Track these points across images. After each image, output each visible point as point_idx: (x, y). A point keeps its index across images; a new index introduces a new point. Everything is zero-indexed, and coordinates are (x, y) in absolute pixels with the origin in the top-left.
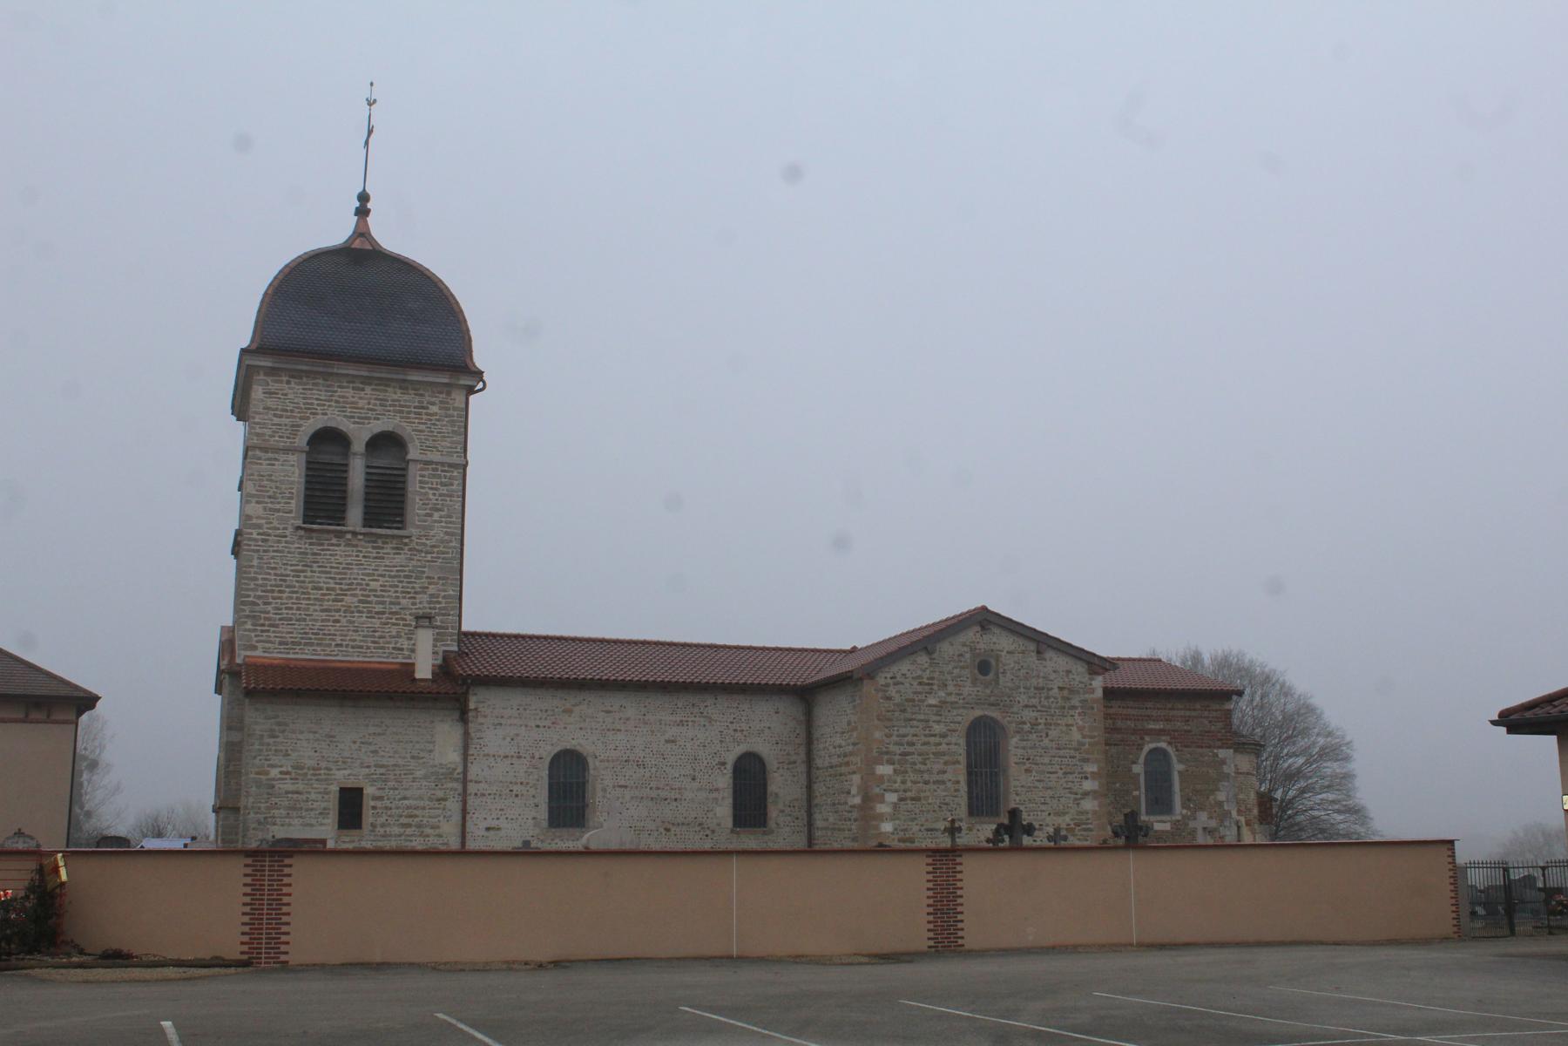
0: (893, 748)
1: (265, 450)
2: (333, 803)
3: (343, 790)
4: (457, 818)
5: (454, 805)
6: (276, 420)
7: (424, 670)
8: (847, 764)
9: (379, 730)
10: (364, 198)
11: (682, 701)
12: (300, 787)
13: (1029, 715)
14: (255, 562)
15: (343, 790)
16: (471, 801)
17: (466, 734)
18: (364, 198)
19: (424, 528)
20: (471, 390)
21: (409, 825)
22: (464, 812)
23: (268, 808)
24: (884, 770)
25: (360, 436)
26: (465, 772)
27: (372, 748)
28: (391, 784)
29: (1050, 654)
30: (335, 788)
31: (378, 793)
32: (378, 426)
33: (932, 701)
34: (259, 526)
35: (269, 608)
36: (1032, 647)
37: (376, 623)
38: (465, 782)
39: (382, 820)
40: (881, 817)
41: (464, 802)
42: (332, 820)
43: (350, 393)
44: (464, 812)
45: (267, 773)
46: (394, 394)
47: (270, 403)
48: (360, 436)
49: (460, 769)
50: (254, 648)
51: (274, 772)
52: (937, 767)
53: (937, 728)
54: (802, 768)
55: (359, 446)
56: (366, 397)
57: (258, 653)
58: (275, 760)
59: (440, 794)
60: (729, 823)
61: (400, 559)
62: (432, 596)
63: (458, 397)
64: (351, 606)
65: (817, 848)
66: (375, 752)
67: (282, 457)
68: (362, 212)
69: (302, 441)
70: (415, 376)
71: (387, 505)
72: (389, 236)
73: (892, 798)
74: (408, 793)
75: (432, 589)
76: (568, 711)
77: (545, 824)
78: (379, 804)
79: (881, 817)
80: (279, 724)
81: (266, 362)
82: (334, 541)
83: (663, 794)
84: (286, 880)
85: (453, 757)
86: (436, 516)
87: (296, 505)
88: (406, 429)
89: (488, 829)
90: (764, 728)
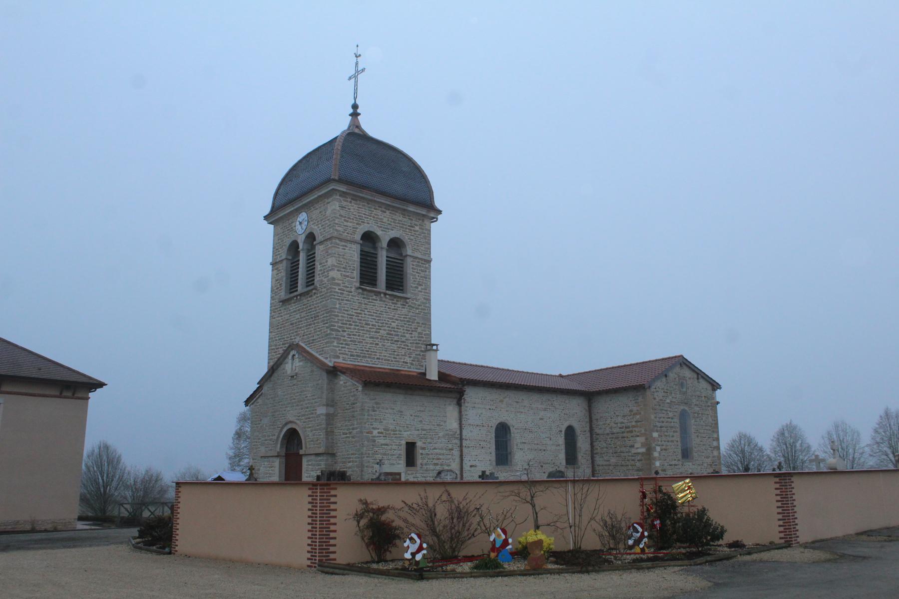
0: (658, 424)
1: (341, 240)
2: (403, 452)
3: (407, 443)
4: (458, 460)
5: (456, 453)
6: (345, 223)
7: (433, 375)
8: (631, 432)
9: (422, 409)
10: (355, 107)
11: (545, 397)
12: (387, 441)
13: (697, 409)
14: (337, 306)
15: (407, 443)
16: (464, 450)
17: (460, 412)
18: (355, 107)
19: (415, 294)
20: (434, 219)
21: (437, 464)
22: (461, 456)
23: (373, 454)
24: (655, 435)
25: (385, 238)
26: (461, 434)
27: (420, 419)
28: (429, 440)
29: (701, 380)
30: (404, 442)
31: (424, 446)
32: (393, 234)
33: (668, 401)
34: (338, 285)
35: (345, 334)
36: (695, 376)
37: (395, 346)
38: (461, 439)
39: (425, 461)
40: (655, 459)
41: (461, 451)
42: (403, 461)
43: (379, 213)
44: (461, 456)
45: (372, 433)
46: (399, 217)
47: (343, 213)
48: (385, 238)
49: (458, 432)
50: (338, 357)
51: (375, 432)
52: (671, 434)
53: (671, 415)
54: (588, 434)
55: (384, 244)
56: (386, 217)
57: (340, 360)
58: (376, 425)
59: (450, 446)
60: (564, 462)
61: (405, 311)
62: (419, 333)
63: (426, 222)
64: (364, 332)
65: (465, 480)
66: (421, 421)
67: (349, 245)
68: (355, 115)
69: (358, 237)
70: (411, 208)
71: (396, 281)
72: (372, 127)
73: (658, 449)
74: (436, 446)
75: (419, 330)
76: (502, 401)
77: (494, 463)
78: (423, 452)
79: (655, 459)
80: (377, 403)
81: (342, 188)
82: (374, 297)
83: (540, 447)
84: (333, 499)
85: (455, 425)
86: (420, 288)
87: (356, 274)
88: (406, 238)
89: (471, 466)
90: (573, 412)
